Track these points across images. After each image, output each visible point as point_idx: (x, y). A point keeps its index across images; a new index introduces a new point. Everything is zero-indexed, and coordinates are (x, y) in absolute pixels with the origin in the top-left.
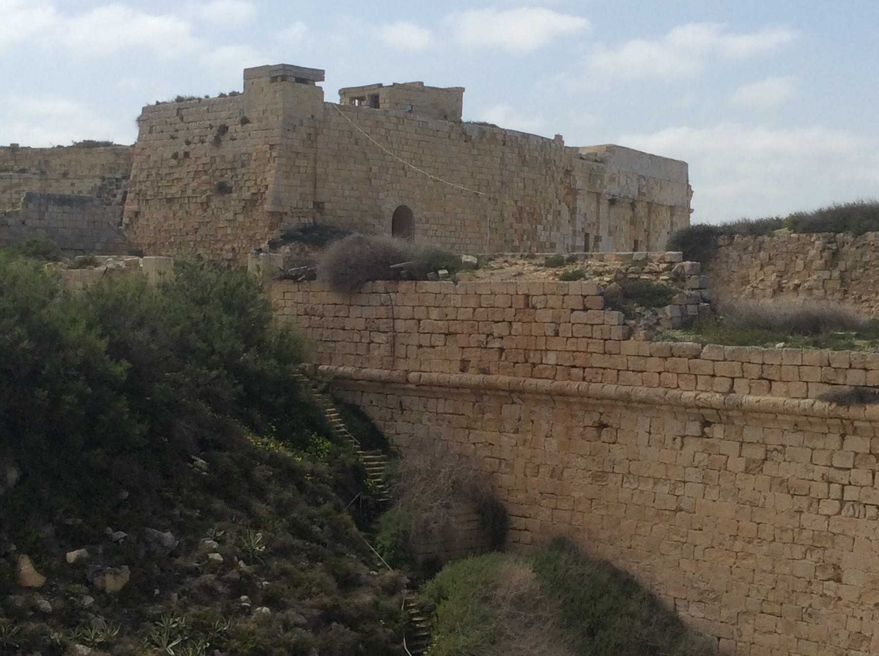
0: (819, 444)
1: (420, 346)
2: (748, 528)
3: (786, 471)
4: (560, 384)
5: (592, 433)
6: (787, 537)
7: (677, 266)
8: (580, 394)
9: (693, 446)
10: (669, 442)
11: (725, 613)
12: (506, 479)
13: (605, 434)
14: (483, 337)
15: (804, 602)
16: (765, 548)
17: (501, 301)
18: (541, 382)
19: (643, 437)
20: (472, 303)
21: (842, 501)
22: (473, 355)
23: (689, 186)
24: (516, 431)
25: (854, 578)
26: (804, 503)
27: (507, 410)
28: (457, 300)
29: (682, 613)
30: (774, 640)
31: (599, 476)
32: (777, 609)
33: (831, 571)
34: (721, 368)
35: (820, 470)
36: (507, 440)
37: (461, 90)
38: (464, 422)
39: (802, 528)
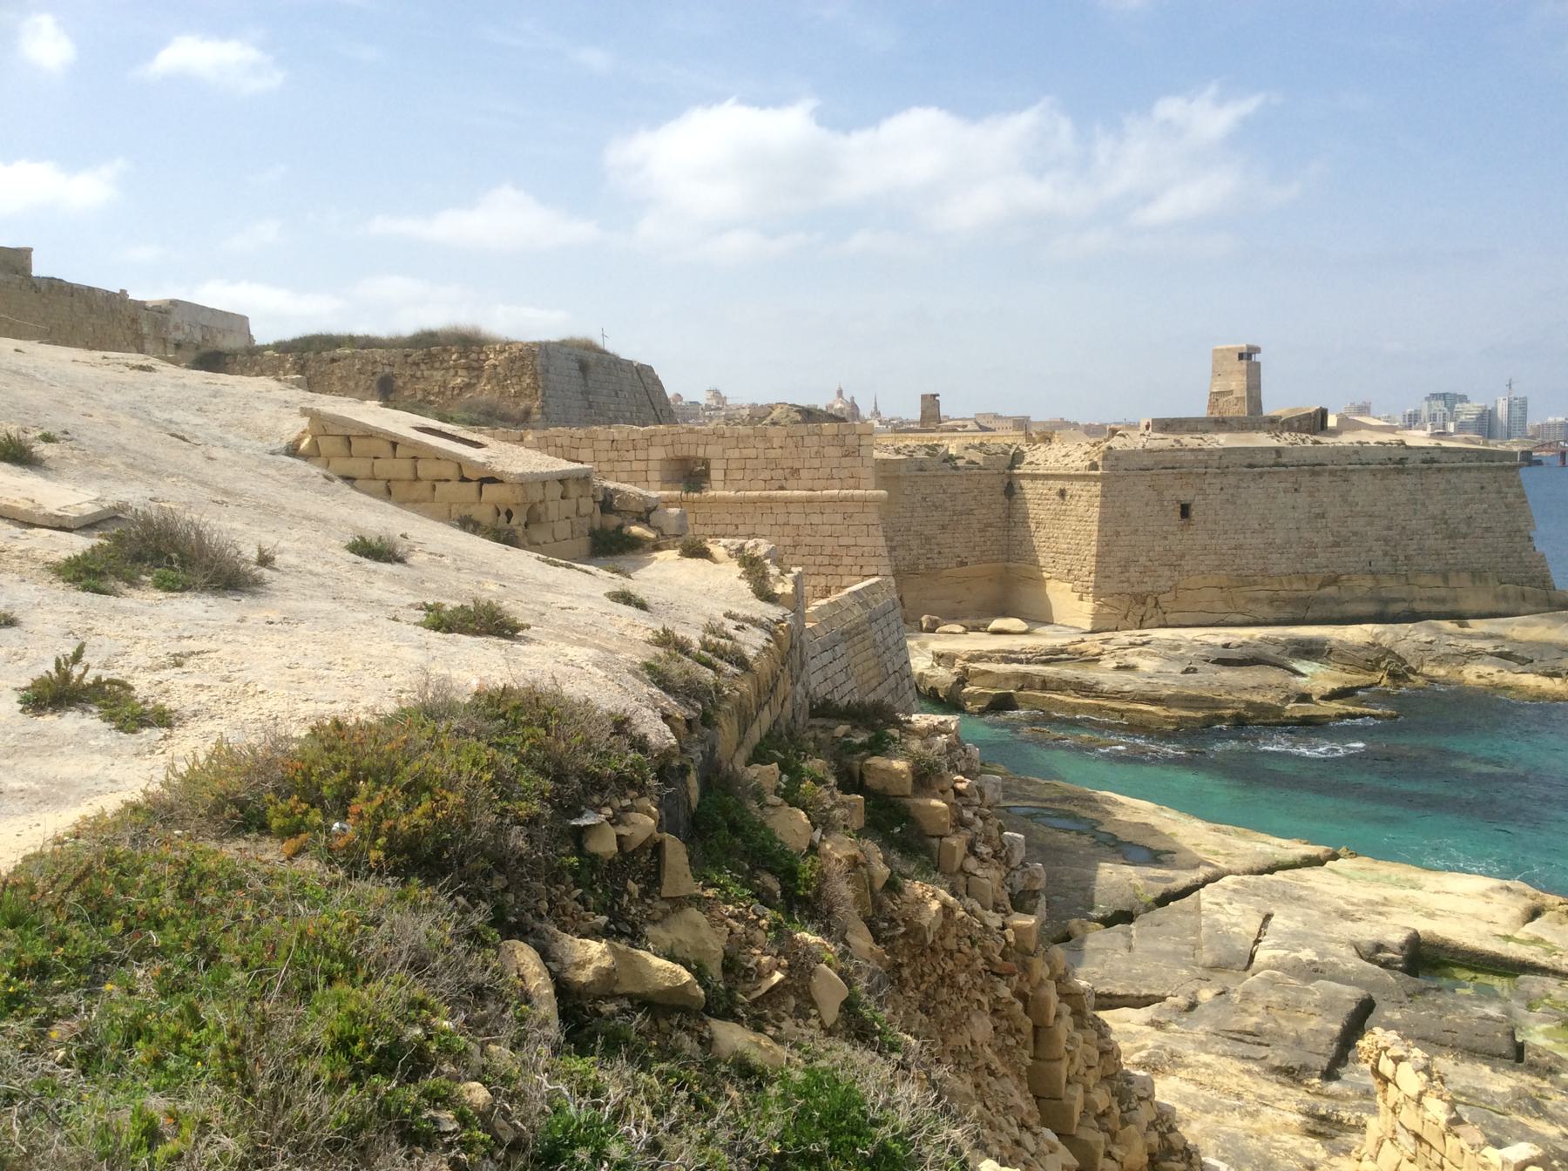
23: (250, 336)
37: (31, 250)
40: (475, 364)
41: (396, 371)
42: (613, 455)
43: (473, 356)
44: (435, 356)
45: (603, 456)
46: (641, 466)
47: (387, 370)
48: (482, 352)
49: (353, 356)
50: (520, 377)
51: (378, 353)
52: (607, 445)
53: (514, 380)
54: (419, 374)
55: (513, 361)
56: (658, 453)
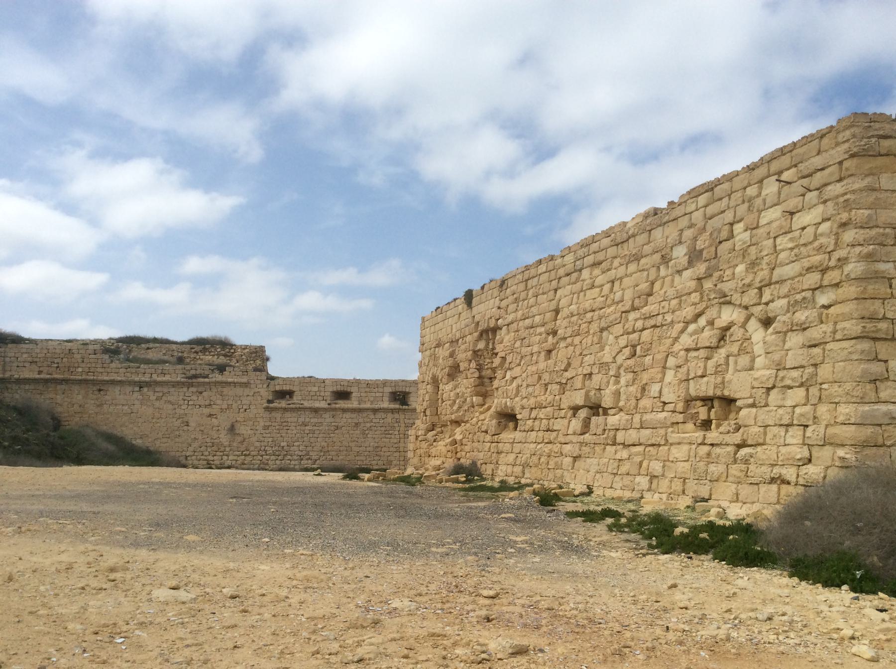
0: (181, 390)
1: (18, 367)
2: (157, 415)
3: (170, 398)
4: (84, 377)
5: (96, 393)
6: (171, 416)
7: (115, 344)
8: (93, 380)
9: (136, 395)
10: (128, 392)
11: (150, 440)
12: (59, 409)
13: (102, 392)
14: (49, 363)
15: (177, 433)
16: (163, 420)
17: (57, 351)
18: (77, 377)
19: (117, 392)
20: (45, 351)
21: (188, 405)
22: (45, 369)
24: (63, 393)
25: (192, 424)
26: (176, 406)
27: (59, 387)
28: (38, 351)
29: (134, 442)
30: (168, 444)
31: (101, 405)
32: (168, 436)
33: (186, 423)
34: (148, 371)
35: (181, 398)
36: (59, 398)
38: (39, 392)
39: (176, 413)
40: (229, 354)
41: (185, 355)
42: (368, 390)
43: (227, 350)
44: (207, 349)
45: (363, 390)
46: (381, 395)
47: (180, 354)
48: (232, 349)
49: (160, 347)
50: (254, 361)
51: (174, 347)
52: (365, 386)
53: (252, 362)
54: (198, 357)
55: (251, 353)
56: (388, 390)
